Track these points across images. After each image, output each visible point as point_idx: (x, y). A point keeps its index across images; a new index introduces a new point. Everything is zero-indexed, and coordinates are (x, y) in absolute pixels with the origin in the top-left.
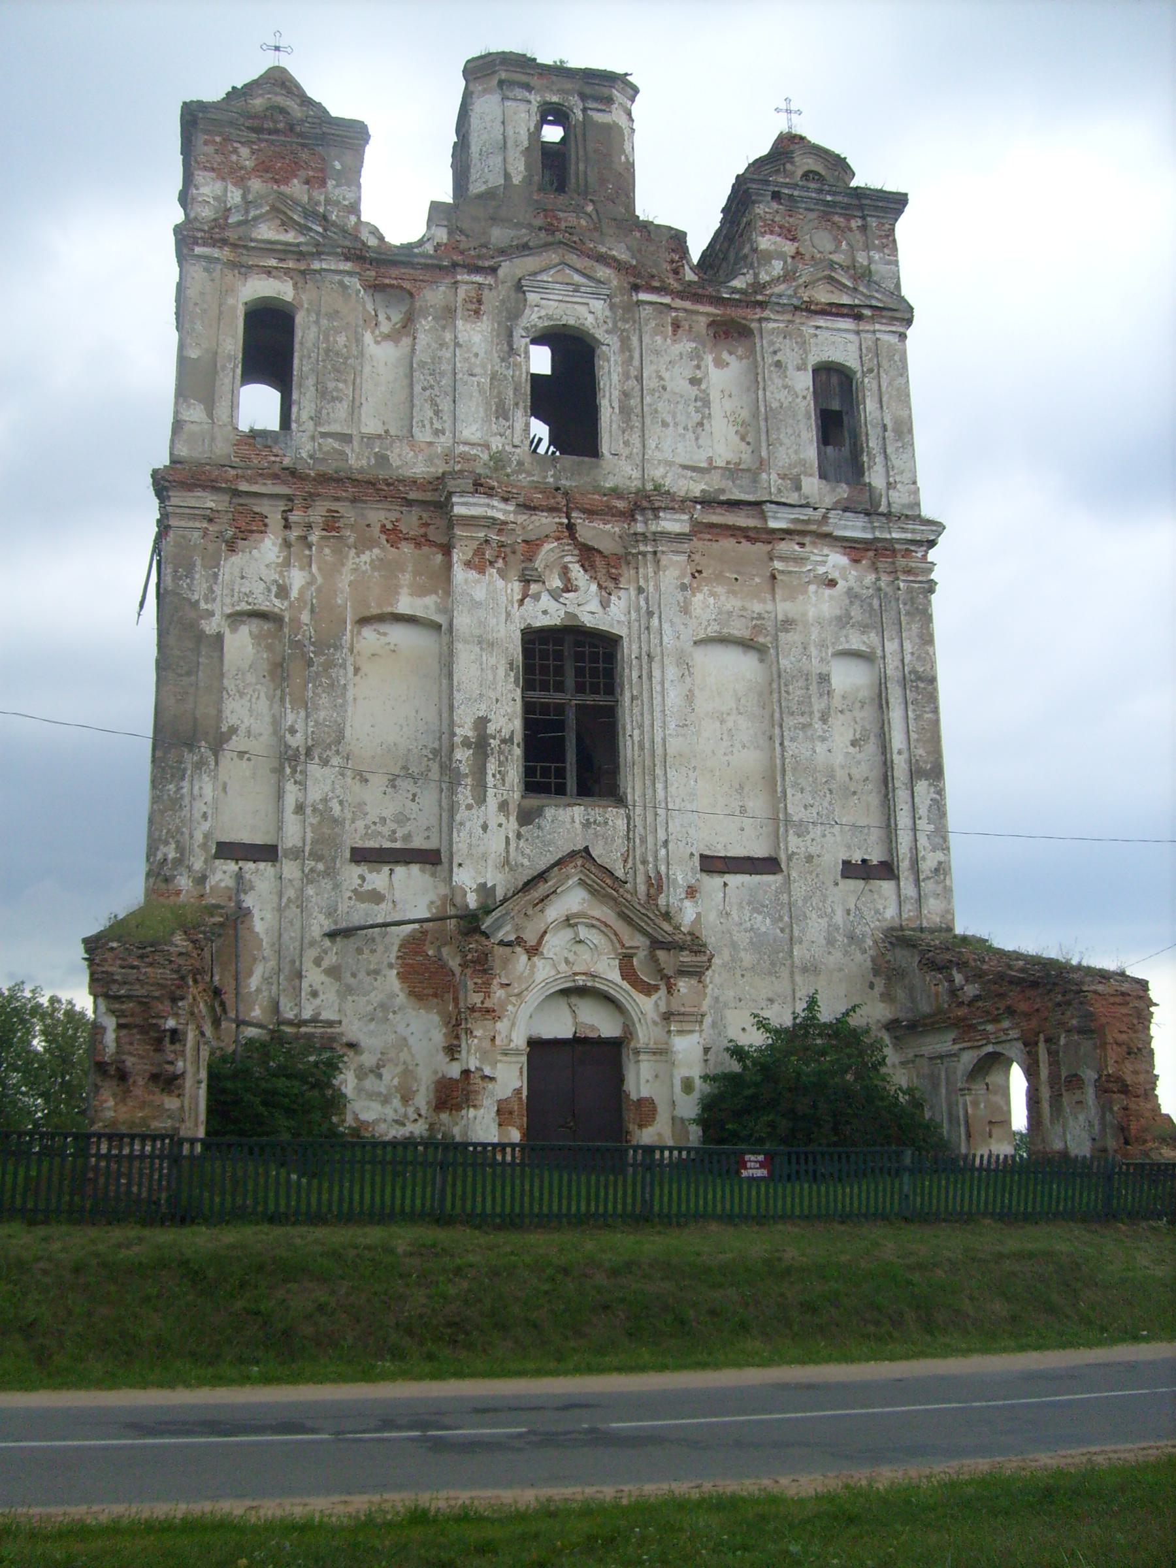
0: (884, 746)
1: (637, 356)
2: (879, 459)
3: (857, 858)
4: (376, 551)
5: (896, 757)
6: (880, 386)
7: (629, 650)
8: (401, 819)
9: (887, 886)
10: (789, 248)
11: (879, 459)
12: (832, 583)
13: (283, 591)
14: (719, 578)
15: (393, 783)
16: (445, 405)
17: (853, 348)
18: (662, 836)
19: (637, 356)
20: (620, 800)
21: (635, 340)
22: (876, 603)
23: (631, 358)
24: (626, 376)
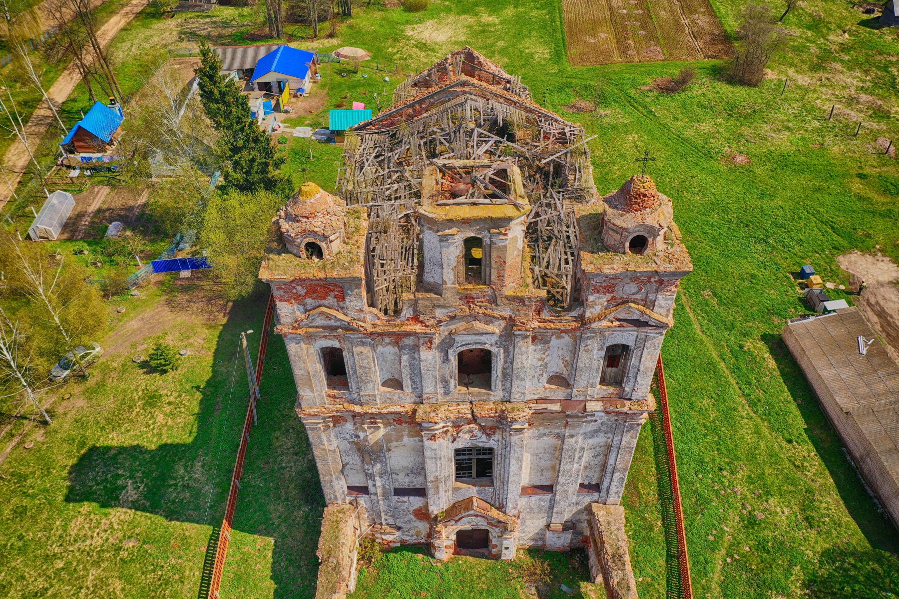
0: (606, 462)
1: (512, 354)
2: (632, 380)
3: (586, 482)
4: (392, 427)
5: (609, 466)
6: (642, 354)
7: (498, 451)
8: (412, 482)
9: (597, 494)
10: (609, 296)
11: (632, 380)
12: (596, 421)
13: (357, 436)
14: (540, 425)
15: (408, 474)
16: (417, 380)
17: (633, 339)
18: (505, 497)
19: (512, 354)
20: (492, 484)
21: (511, 348)
22: (614, 426)
23: (509, 355)
24: (505, 362)
